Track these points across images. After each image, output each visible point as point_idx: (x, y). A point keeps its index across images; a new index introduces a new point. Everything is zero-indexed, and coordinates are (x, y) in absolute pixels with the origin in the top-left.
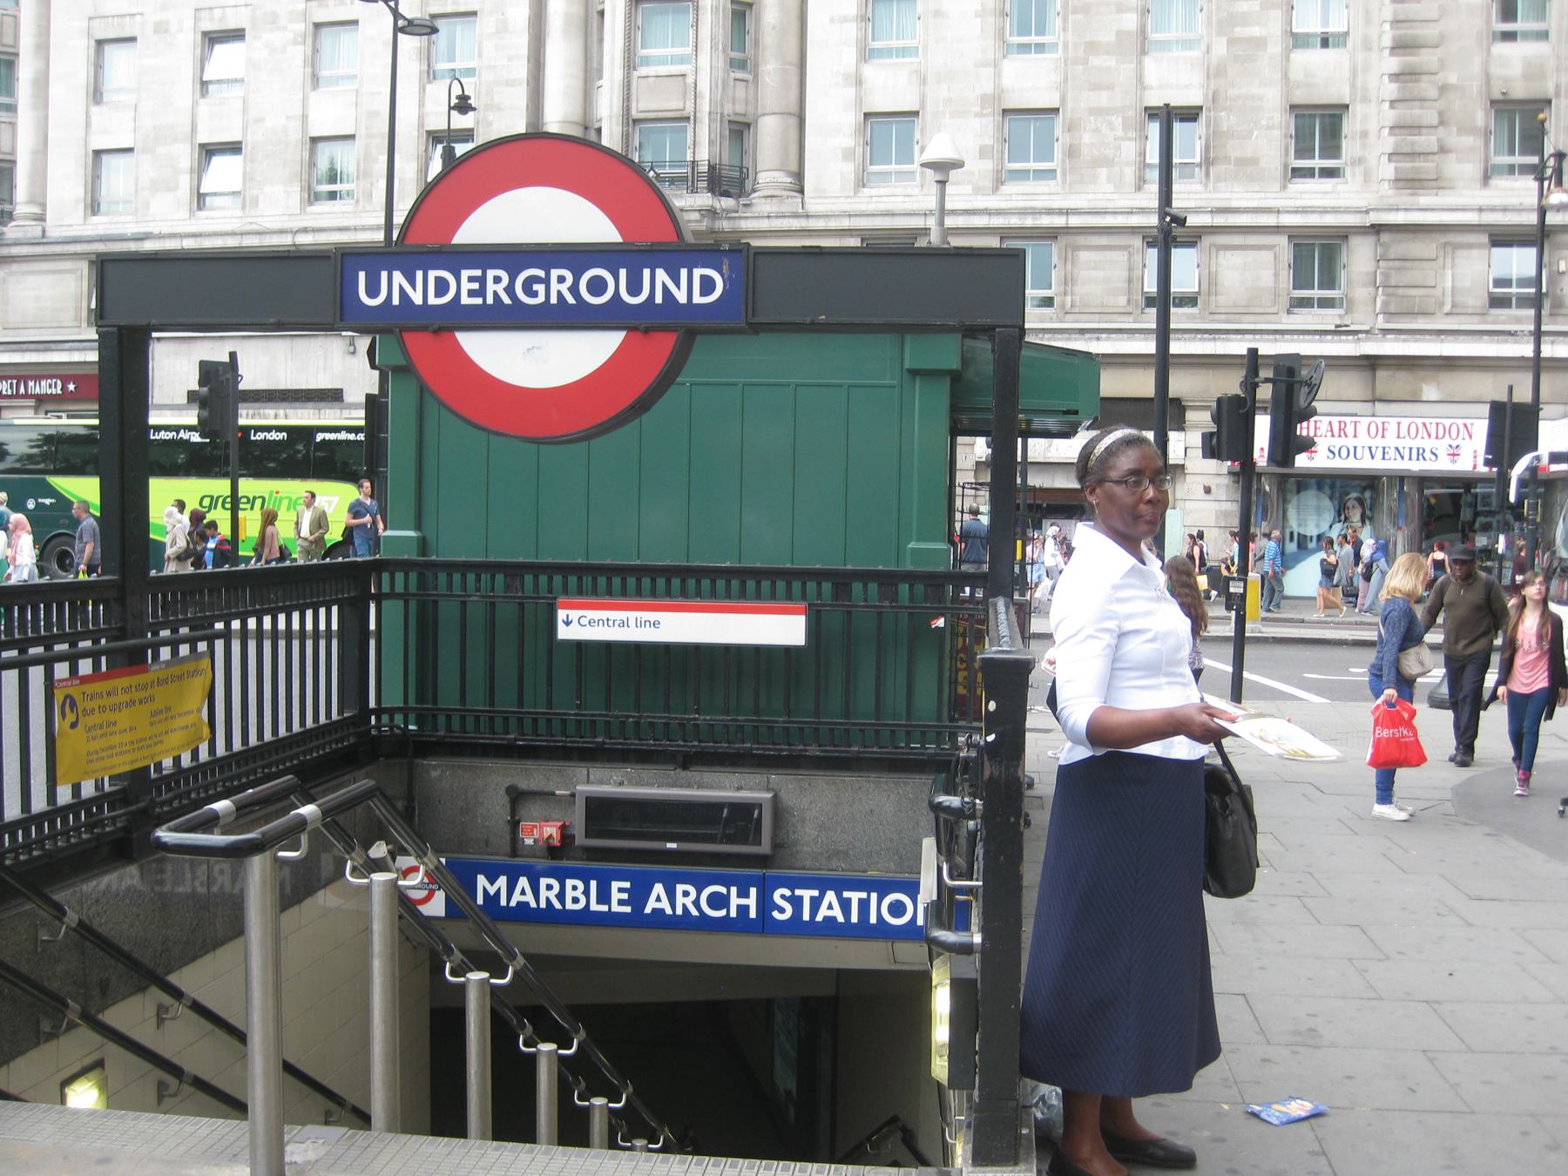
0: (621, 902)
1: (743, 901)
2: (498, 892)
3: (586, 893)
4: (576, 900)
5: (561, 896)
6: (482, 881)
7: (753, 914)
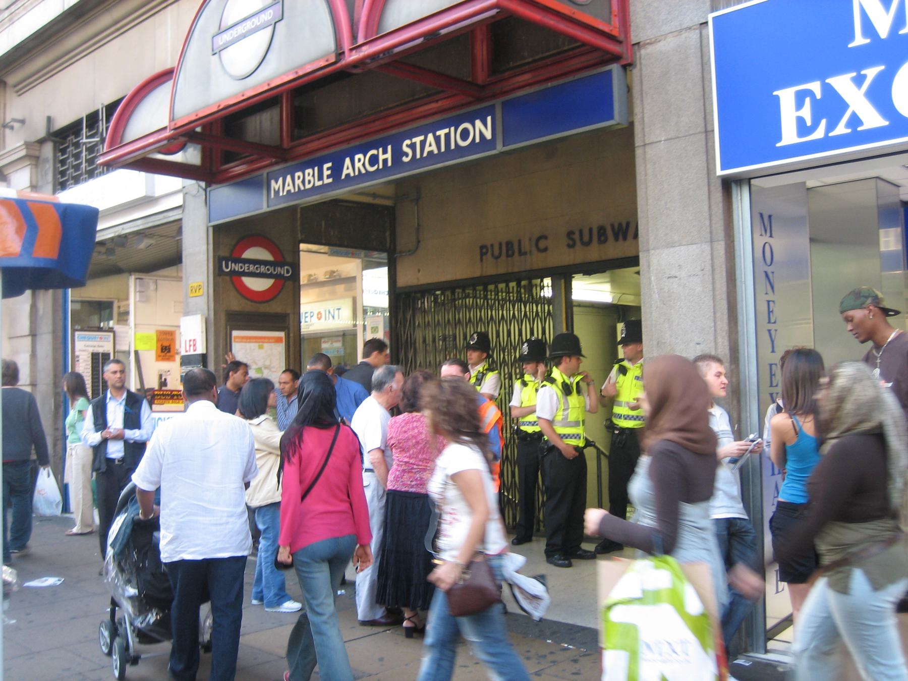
0: (328, 177)
5: (303, 182)
7: (390, 164)
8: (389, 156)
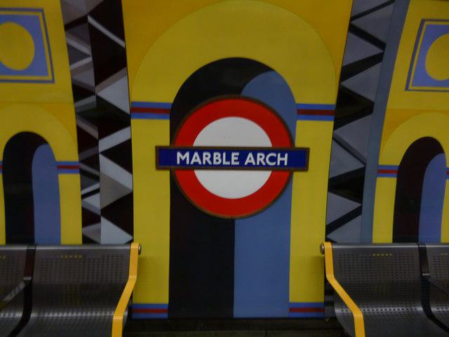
0: (235, 161)
1: (282, 159)
2: (186, 159)
3: (222, 157)
4: (217, 161)
5: (212, 159)
6: (179, 155)
7: (286, 164)
8: (286, 159)
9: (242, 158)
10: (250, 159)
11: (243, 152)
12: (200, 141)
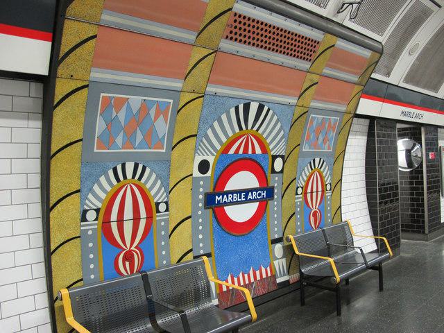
5: (232, 199)
6: (217, 197)
8: (265, 194)
9: (246, 196)
10: (250, 197)
11: (247, 191)
12: (228, 187)
